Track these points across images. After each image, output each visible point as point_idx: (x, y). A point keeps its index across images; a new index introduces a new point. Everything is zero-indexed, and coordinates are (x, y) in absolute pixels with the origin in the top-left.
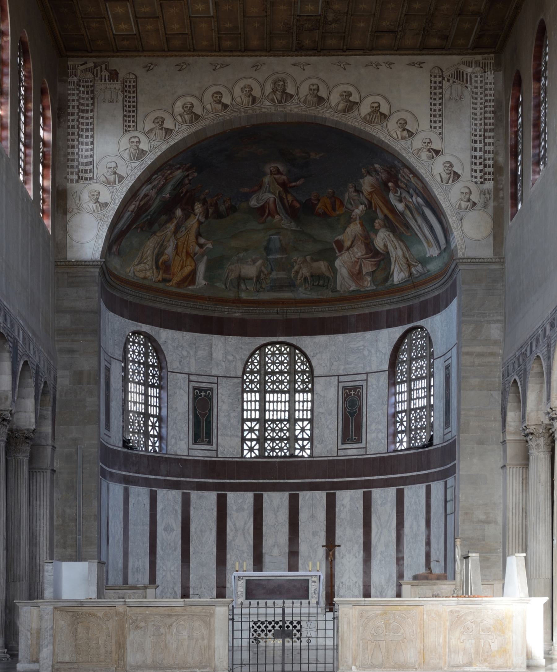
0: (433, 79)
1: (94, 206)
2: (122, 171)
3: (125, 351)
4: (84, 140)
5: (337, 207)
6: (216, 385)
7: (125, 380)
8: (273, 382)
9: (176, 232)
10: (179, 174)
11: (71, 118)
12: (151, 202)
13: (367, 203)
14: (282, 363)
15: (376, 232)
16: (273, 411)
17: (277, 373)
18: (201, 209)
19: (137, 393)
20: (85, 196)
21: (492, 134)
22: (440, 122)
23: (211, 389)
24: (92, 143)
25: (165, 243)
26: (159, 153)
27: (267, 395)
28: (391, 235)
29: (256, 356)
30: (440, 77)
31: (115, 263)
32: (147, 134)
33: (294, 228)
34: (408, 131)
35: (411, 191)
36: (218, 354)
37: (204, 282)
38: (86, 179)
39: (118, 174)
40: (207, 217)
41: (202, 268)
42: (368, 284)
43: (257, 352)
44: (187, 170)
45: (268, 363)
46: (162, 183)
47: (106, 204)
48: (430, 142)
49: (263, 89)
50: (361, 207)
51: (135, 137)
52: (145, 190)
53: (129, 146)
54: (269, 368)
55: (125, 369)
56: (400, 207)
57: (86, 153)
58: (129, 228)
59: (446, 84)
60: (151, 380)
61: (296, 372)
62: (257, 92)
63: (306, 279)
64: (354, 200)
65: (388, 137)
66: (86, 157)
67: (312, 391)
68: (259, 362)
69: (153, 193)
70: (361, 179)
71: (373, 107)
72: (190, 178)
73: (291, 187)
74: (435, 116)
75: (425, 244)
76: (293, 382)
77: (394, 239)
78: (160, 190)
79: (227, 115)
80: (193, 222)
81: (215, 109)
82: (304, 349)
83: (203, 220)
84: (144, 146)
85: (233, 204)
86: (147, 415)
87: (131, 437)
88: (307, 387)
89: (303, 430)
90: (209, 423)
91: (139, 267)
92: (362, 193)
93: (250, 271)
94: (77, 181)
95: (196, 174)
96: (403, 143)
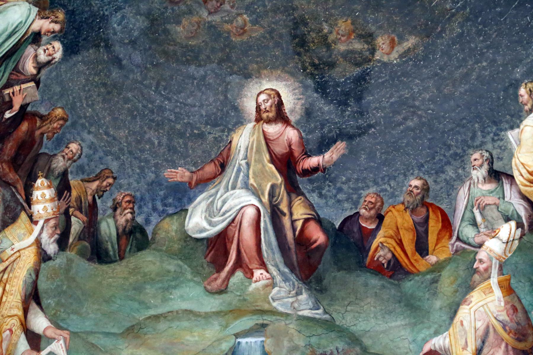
5: (432, 238)
13: (523, 213)
18: (50, 206)
33: (307, 313)
64: (482, 209)
70: (512, 128)
73: (307, 173)
83: (51, 248)
85: (140, 220)
92: (511, 177)
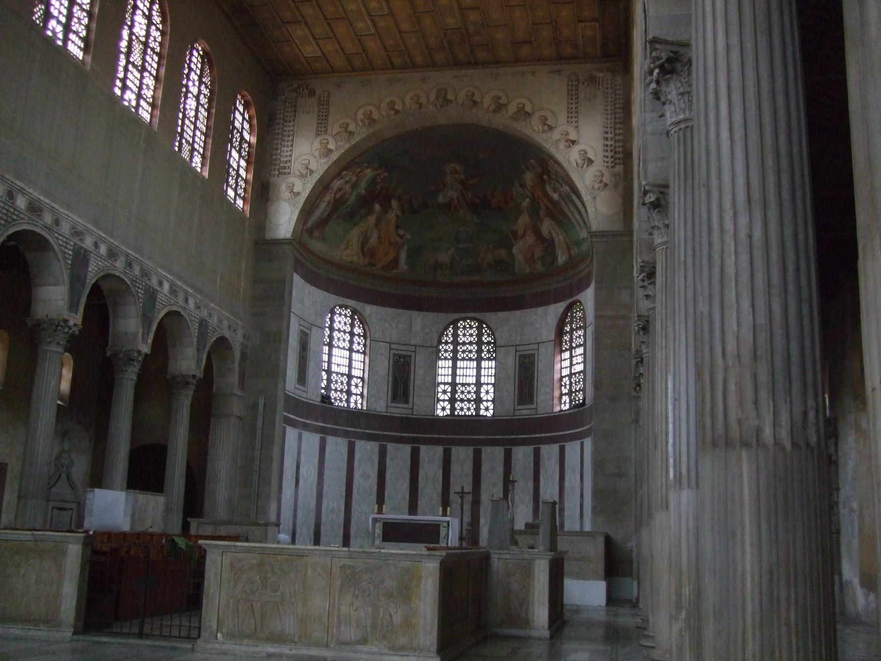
0: (570, 84)
1: (289, 195)
2: (313, 166)
4: (286, 144)
6: (414, 353)
8: (464, 352)
9: (377, 223)
10: (369, 173)
11: (277, 127)
12: (347, 196)
14: (471, 335)
15: (542, 221)
16: (463, 376)
17: (467, 344)
19: (341, 357)
20: (283, 188)
21: (621, 126)
22: (576, 117)
23: (410, 357)
24: (292, 146)
25: (368, 233)
26: (343, 151)
27: (459, 362)
28: (554, 223)
29: (450, 329)
30: (576, 81)
31: (317, 246)
32: (334, 137)
34: (549, 126)
35: (560, 180)
36: (417, 326)
37: (406, 267)
38: (285, 174)
39: (310, 169)
40: (403, 213)
41: (403, 256)
42: (539, 267)
43: (451, 326)
44: (377, 169)
45: (459, 335)
46: (355, 179)
47: (299, 193)
48: (567, 134)
49: (428, 97)
50: (527, 200)
51: (325, 139)
52: (337, 184)
53: (319, 146)
54: (461, 339)
56: (556, 197)
57: (286, 154)
58: (329, 217)
59: (581, 87)
60: (356, 347)
61: (483, 343)
62: (423, 100)
65: (531, 131)
66: (286, 156)
67: (495, 359)
68: (452, 335)
69: (347, 187)
71: (518, 107)
72: (382, 177)
74: (571, 113)
75: (578, 228)
77: (556, 227)
78: (354, 186)
80: (391, 216)
81: (389, 114)
82: (489, 324)
83: (399, 213)
84: (331, 146)
86: (350, 376)
88: (492, 355)
89: (487, 392)
91: (345, 253)
93: (444, 257)
94: (278, 176)
95: (386, 174)
96: (544, 135)
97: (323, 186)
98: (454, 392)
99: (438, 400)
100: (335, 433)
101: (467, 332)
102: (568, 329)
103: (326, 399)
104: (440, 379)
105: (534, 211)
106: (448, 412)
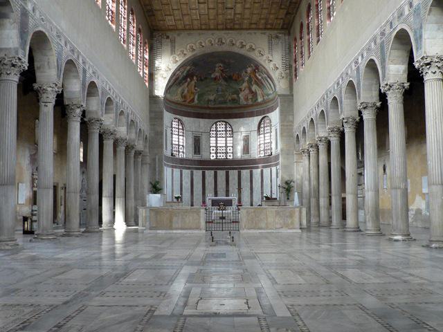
3: (172, 124)
7: (172, 134)
10: (188, 68)
31: (168, 96)
32: (178, 55)
36: (202, 125)
41: (196, 97)
42: (250, 102)
55: (172, 130)
56: (260, 78)
60: (180, 134)
63: (230, 101)
67: (232, 137)
76: (226, 134)
79: (203, 49)
80: (193, 82)
86: (179, 145)
87: (174, 153)
90: (199, 148)
93: (212, 98)
97: (174, 74)
98: (217, 150)
99: (210, 153)
100: (176, 167)
101: (221, 127)
102: (262, 126)
103: (172, 154)
104: (211, 145)
105: (250, 81)
106: (215, 157)
